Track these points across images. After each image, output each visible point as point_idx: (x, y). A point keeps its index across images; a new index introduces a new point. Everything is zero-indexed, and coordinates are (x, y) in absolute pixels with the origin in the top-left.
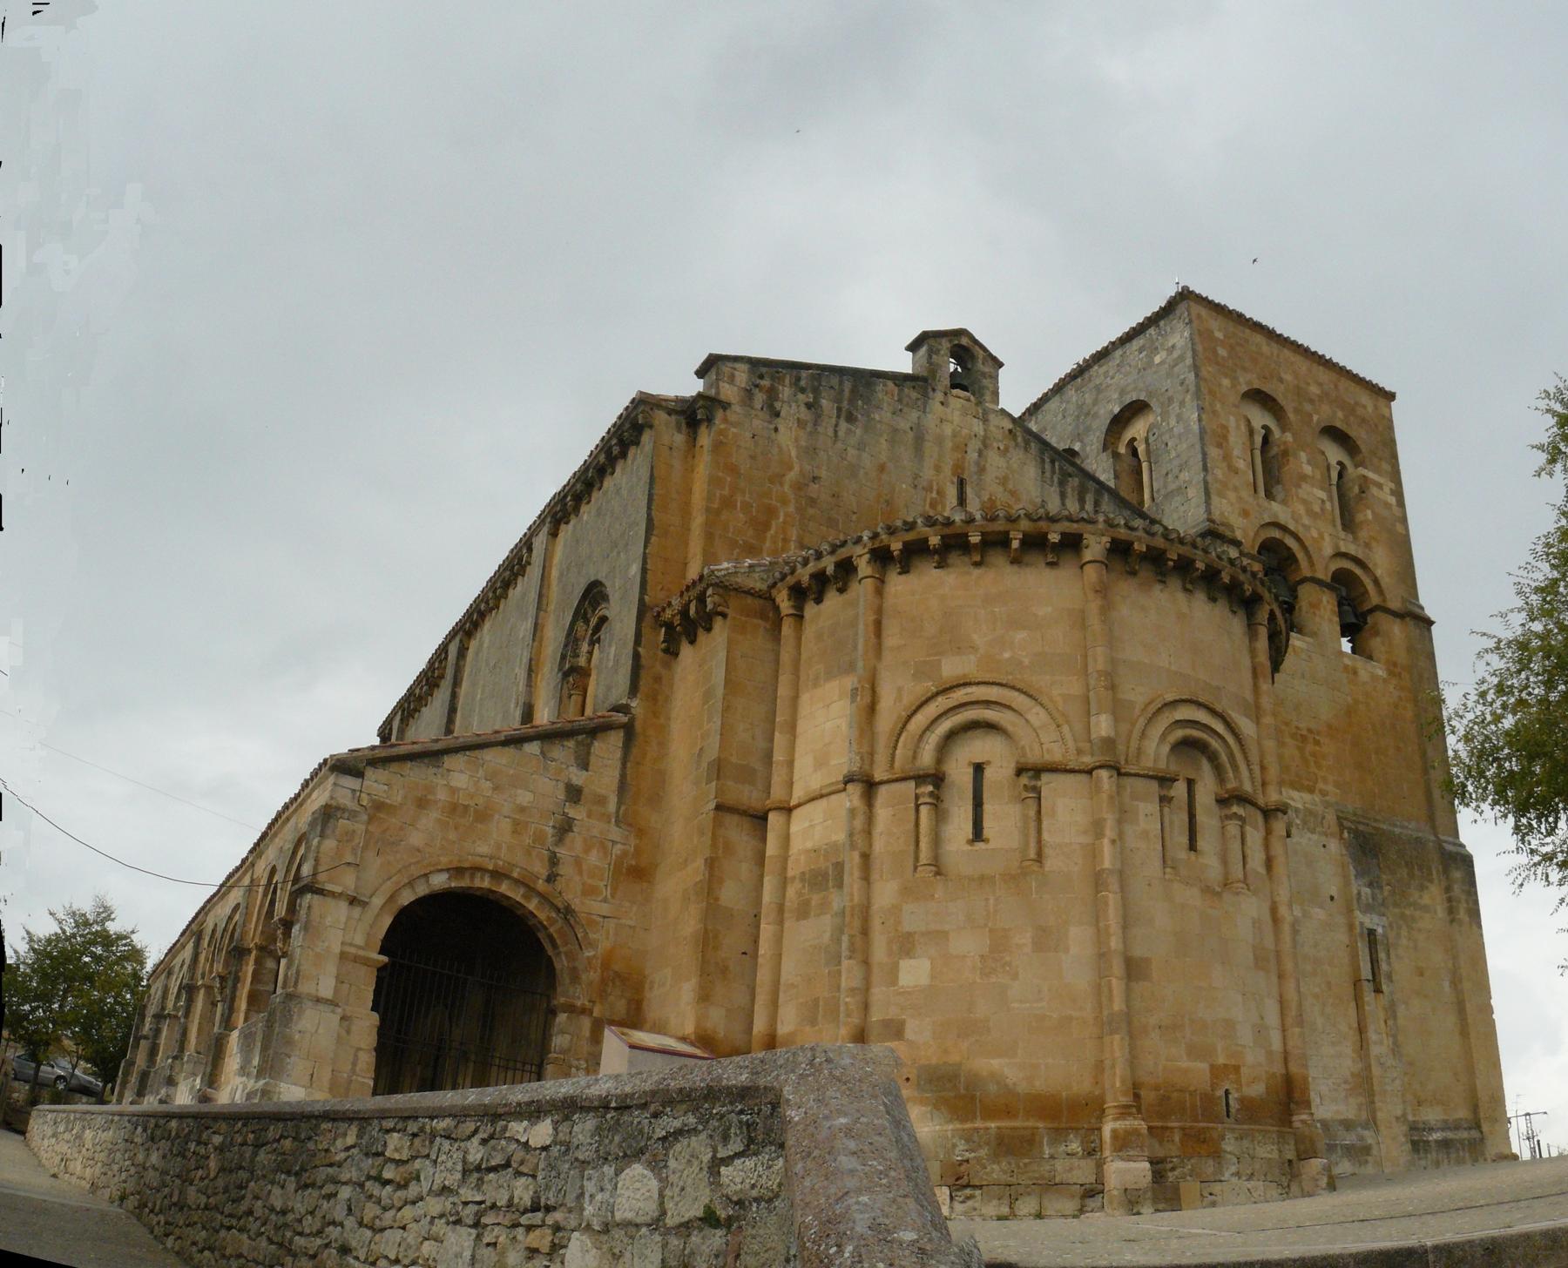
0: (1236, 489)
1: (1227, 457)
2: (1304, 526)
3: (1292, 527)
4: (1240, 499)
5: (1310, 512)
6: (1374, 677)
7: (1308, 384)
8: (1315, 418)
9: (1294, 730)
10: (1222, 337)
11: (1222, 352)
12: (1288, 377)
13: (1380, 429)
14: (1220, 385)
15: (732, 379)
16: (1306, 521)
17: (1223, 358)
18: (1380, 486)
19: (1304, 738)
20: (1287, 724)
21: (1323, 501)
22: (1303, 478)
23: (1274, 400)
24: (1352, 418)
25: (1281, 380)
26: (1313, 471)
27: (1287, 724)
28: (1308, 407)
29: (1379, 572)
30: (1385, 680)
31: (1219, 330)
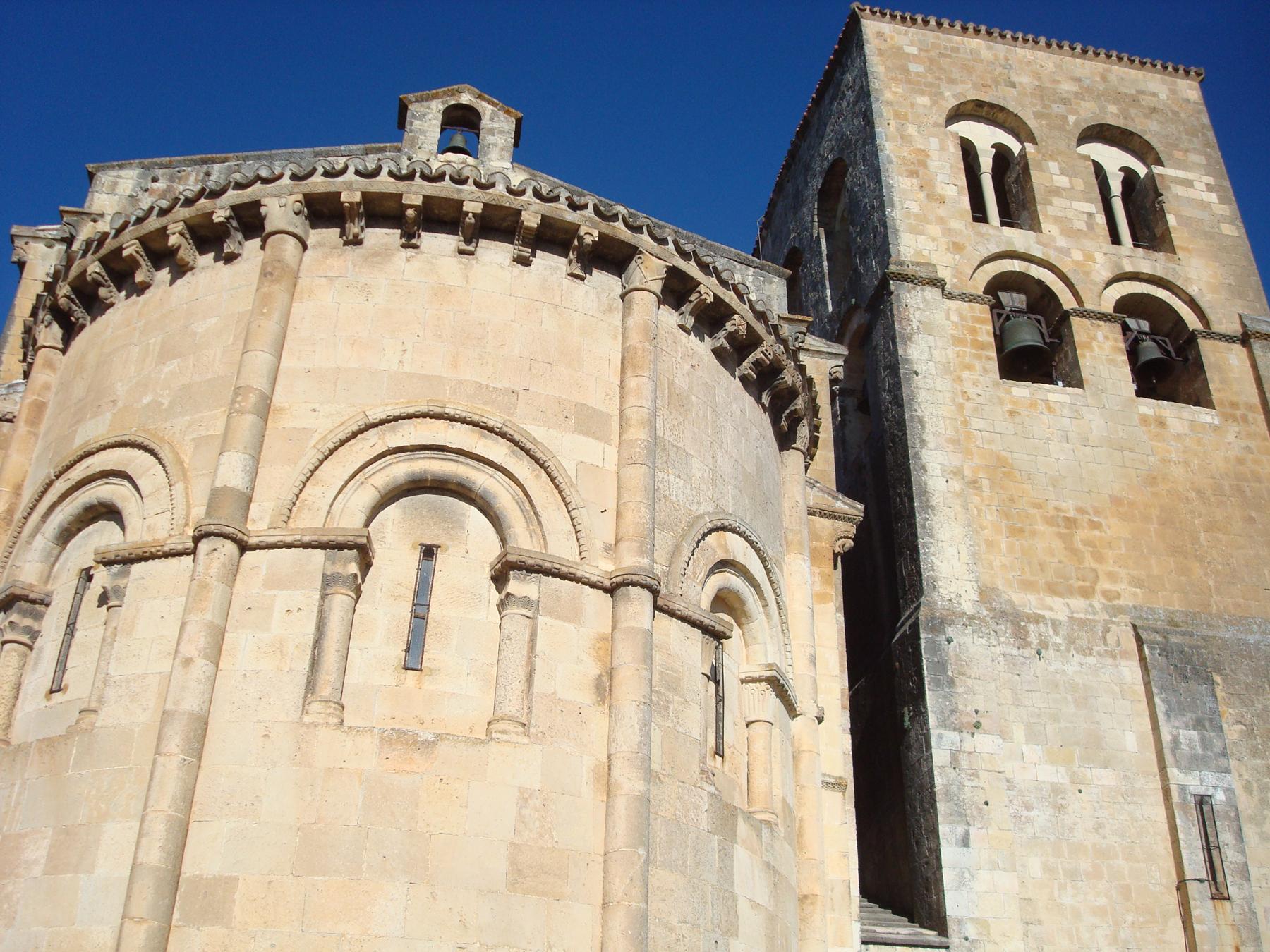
0: (941, 220)
1: (927, 187)
2: (1057, 249)
3: (1037, 252)
4: (948, 231)
5: (1069, 232)
6: (1193, 424)
7: (1059, 82)
8: (1072, 119)
9: (1052, 513)
10: (916, 53)
11: (915, 68)
12: (1024, 80)
13: (1182, 115)
14: (913, 105)
15: (112, 190)
16: (1062, 242)
17: (918, 75)
18: (1188, 184)
19: (1071, 523)
20: (1039, 506)
21: (1090, 215)
22: (1057, 191)
23: (1002, 109)
24: (1133, 111)
25: (1013, 85)
26: (1071, 182)
27: (1039, 506)
28: (1057, 109)
29: (1193, 290)
30: (1216, 429)
31: (912, 45)
